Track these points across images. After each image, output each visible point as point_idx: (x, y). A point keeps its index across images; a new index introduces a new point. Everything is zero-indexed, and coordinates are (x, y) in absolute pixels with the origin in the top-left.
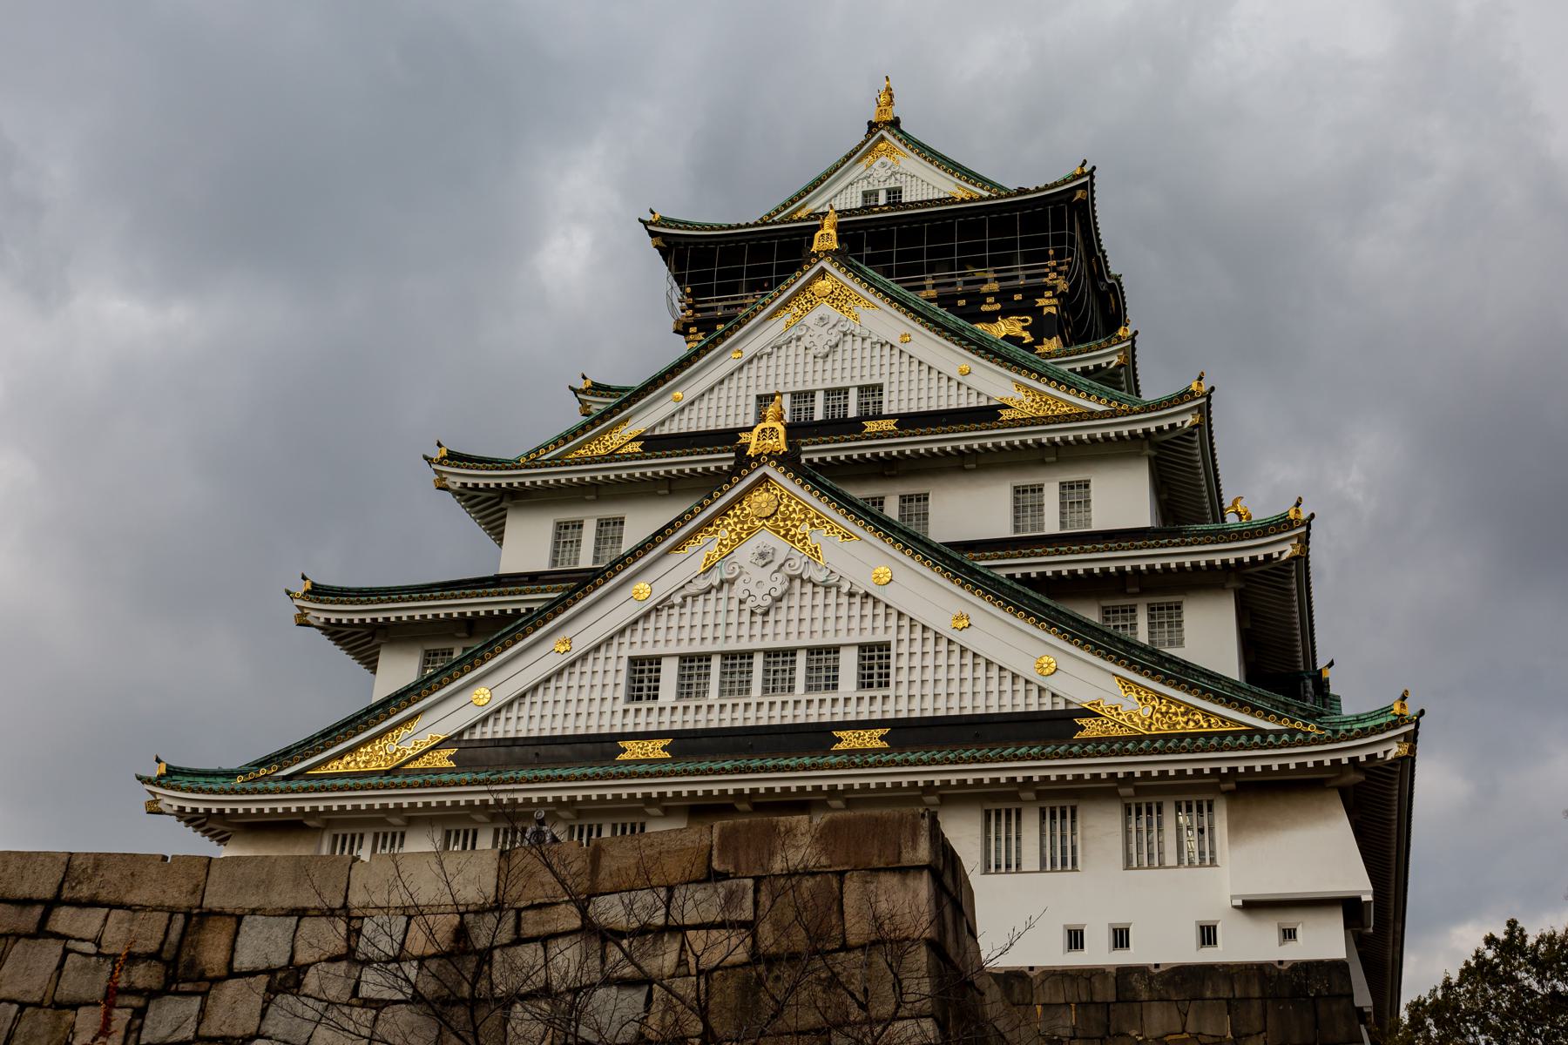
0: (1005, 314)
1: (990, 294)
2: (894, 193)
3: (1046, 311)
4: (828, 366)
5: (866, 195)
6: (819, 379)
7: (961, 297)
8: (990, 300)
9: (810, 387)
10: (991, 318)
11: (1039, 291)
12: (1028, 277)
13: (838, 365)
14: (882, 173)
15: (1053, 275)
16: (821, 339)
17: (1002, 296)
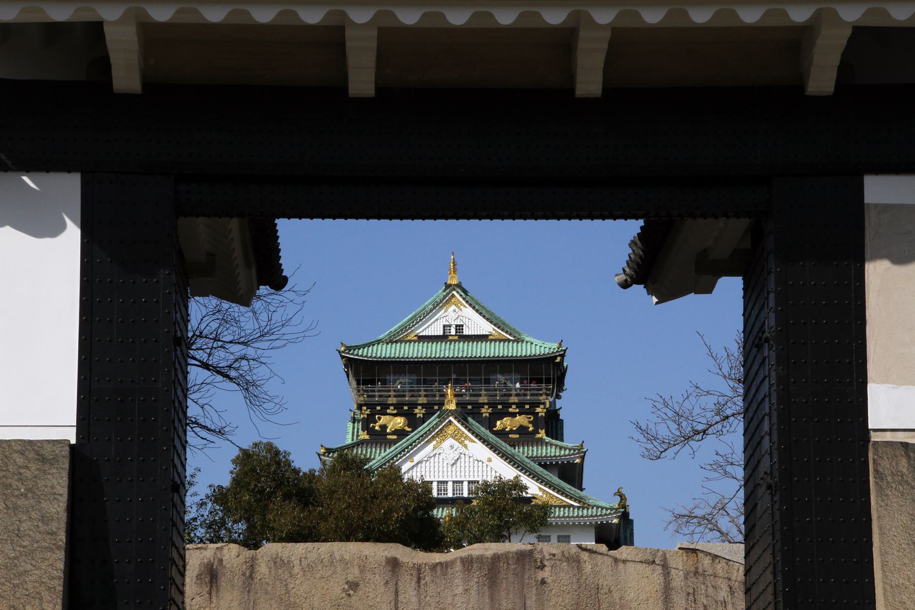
0: (520, 414)
1: (514, 404)
2: (459, 328)
3: (540, 415)
4: (454, 469)
5: (444, 326)
6: (450, 476)
7: (500, 404)
8: (514, 406)
9: (445, 479)
10: (513, 415)
11: (538, 404)
12: (532, 395)
13: (458, 469)
14: (454, 315)
15: (544, 397)
16: (452, 456)
17: (520, 405)
